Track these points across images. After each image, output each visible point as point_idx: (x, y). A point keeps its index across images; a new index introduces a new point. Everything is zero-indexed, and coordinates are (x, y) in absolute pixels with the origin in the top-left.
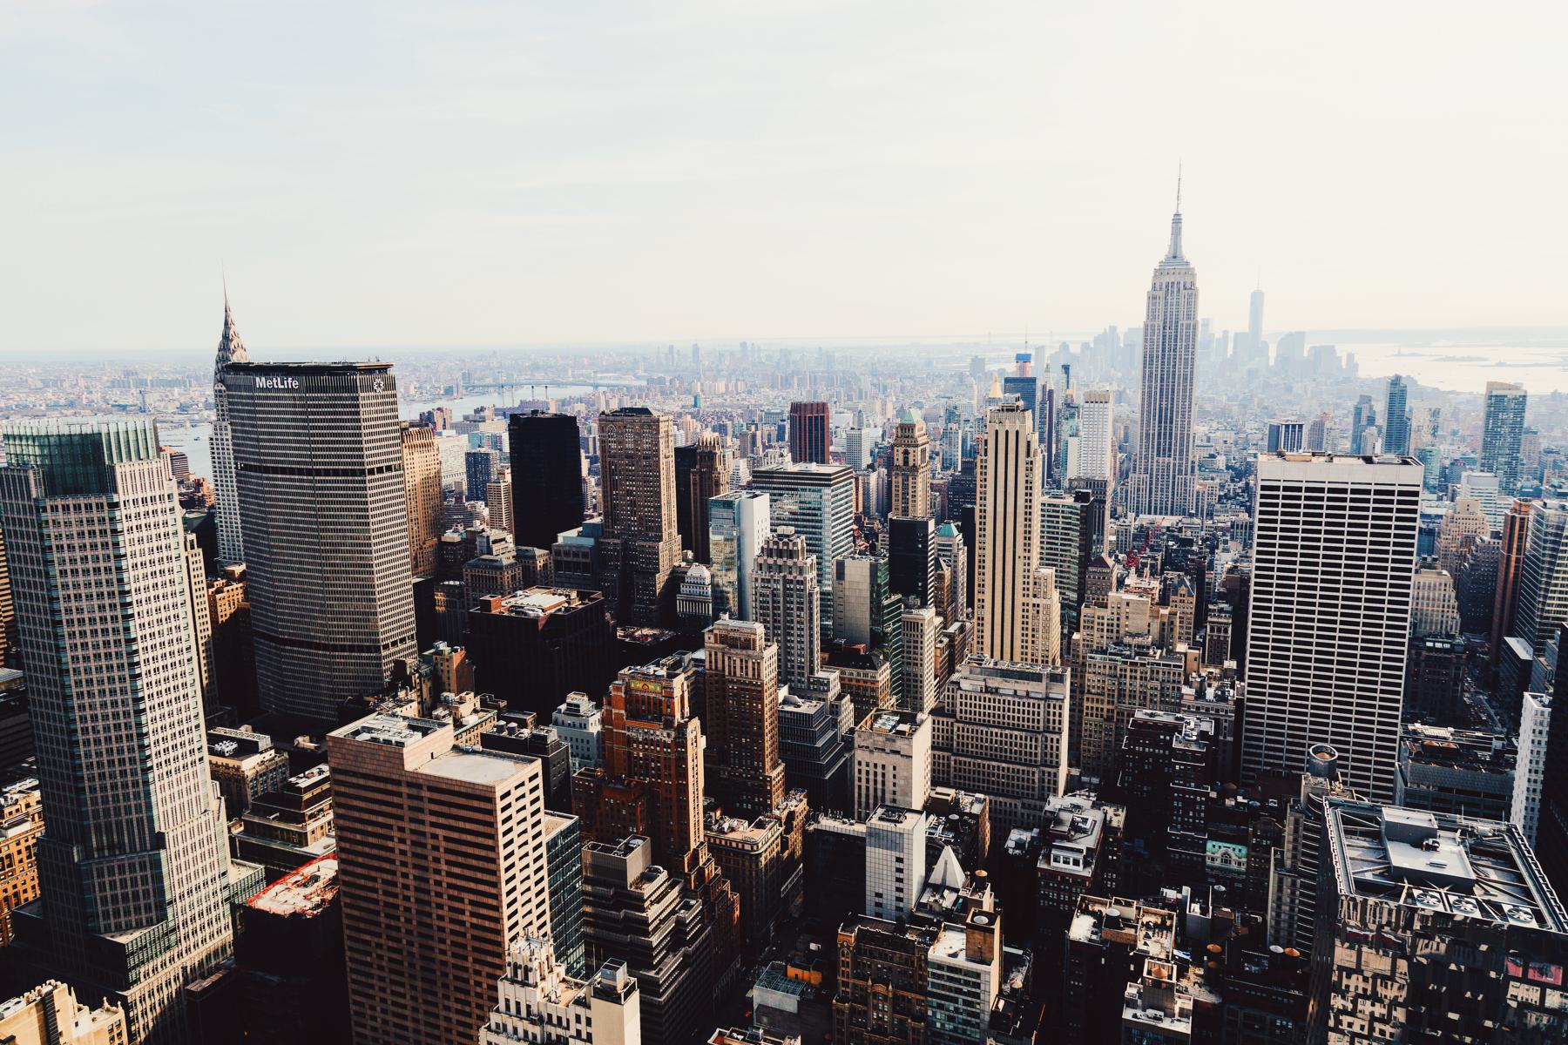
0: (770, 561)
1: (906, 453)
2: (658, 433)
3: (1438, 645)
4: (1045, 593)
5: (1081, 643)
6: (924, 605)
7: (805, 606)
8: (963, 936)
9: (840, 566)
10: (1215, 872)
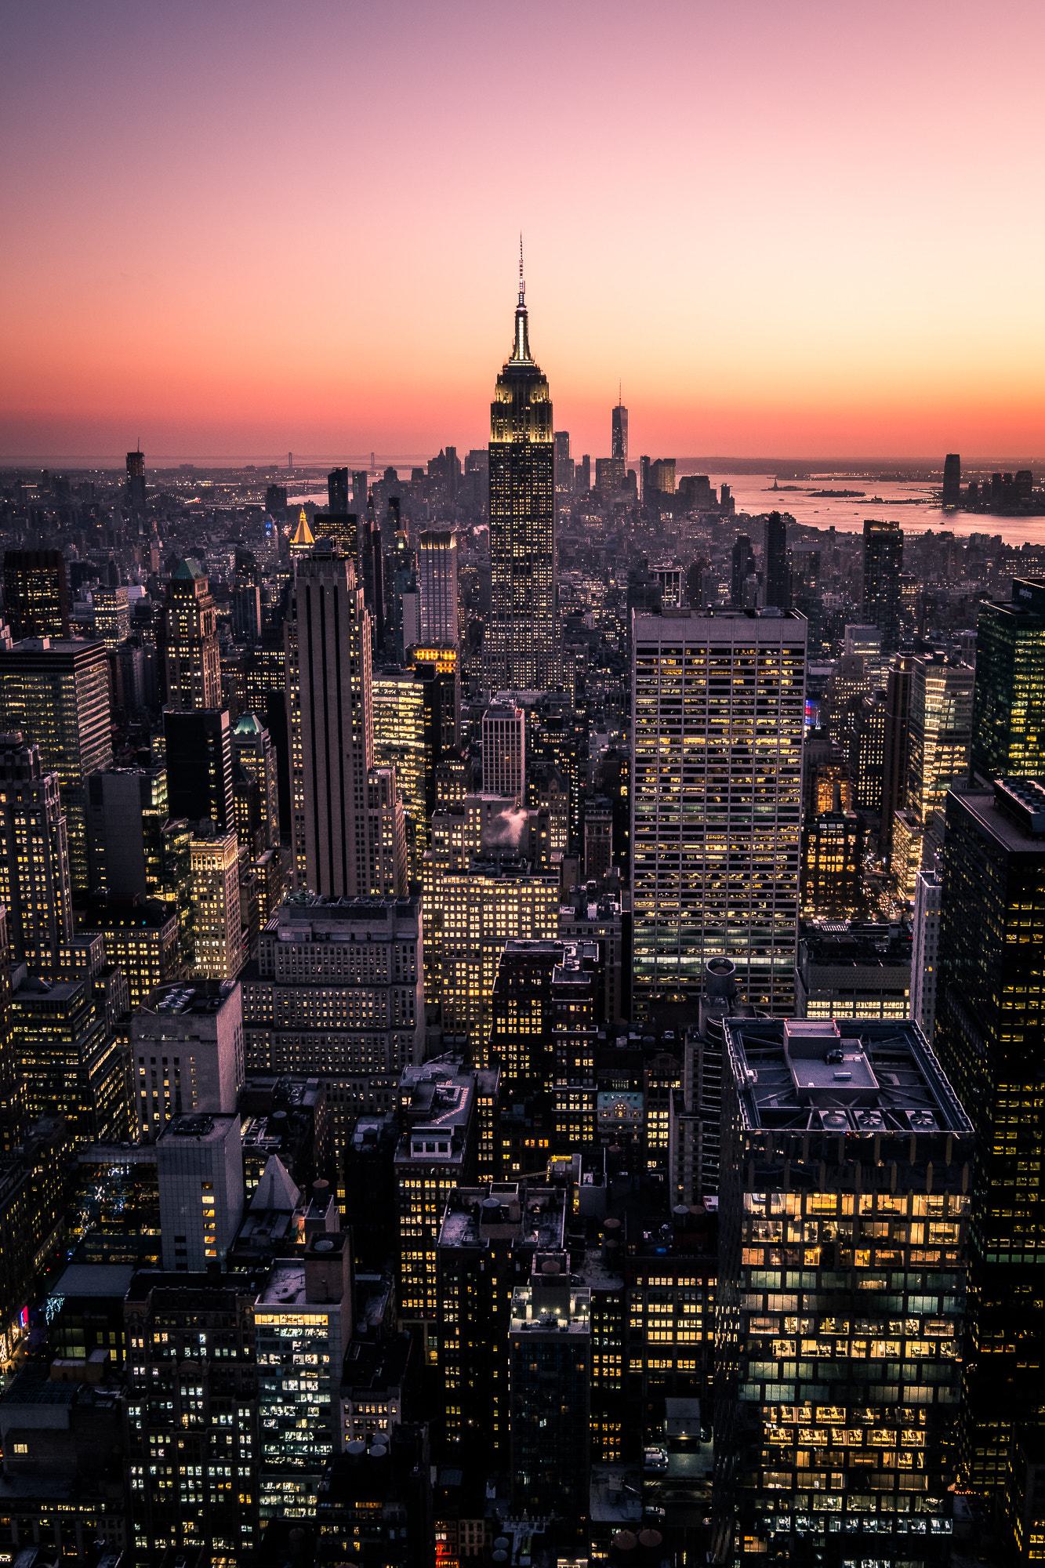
8: (302, 1272)
10: (607, 1131)
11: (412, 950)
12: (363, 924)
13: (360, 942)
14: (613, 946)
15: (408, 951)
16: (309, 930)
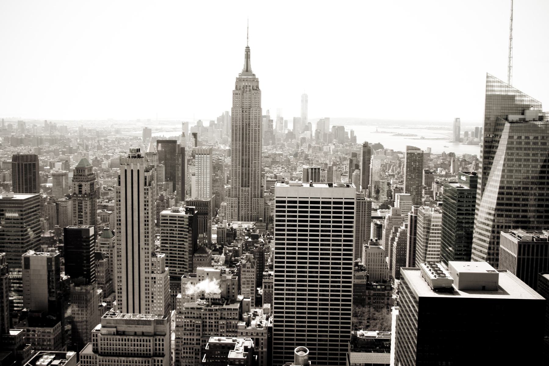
1: (80, 186)
11: (163, 340)
12: (140, 327)
13: (139, 336)
14: (262, 341)
15: (161, 340)
16: (115, 329)
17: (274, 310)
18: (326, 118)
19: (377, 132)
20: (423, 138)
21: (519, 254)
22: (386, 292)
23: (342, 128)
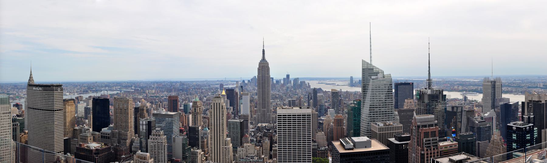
0: (154, 137)
1: (195, 109)
2: (128, 103)
3: (323, 149)
4: (228, 144)
5: (238, 157)
6: (198, 149)
7: (163, 149)
9: (174, 138)
17: (278, 161)
18: (297, 78)
19: (319, 83)
20: (338, 85)
21: (379, 132)
22: (326, 151)
23: (304, 82)
